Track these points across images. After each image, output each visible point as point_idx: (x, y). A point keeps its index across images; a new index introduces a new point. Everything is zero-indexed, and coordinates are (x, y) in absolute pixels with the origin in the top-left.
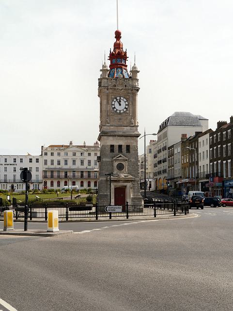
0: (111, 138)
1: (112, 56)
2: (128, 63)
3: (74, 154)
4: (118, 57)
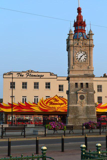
1: (76, 25)
2: (86, 29)
4: (79, 24)
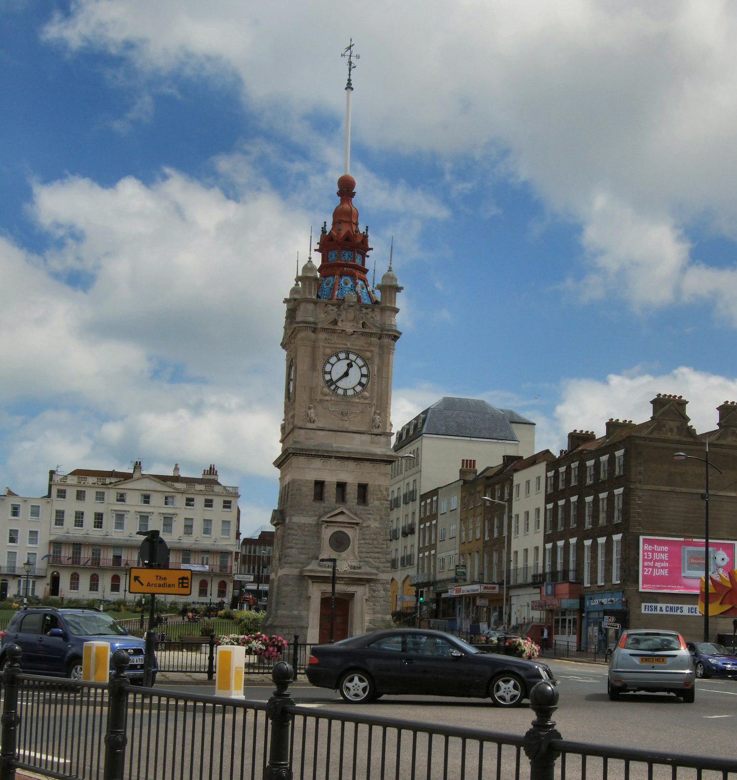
0: (317, 463)
2: (369, 263)
3: (146, 499)
